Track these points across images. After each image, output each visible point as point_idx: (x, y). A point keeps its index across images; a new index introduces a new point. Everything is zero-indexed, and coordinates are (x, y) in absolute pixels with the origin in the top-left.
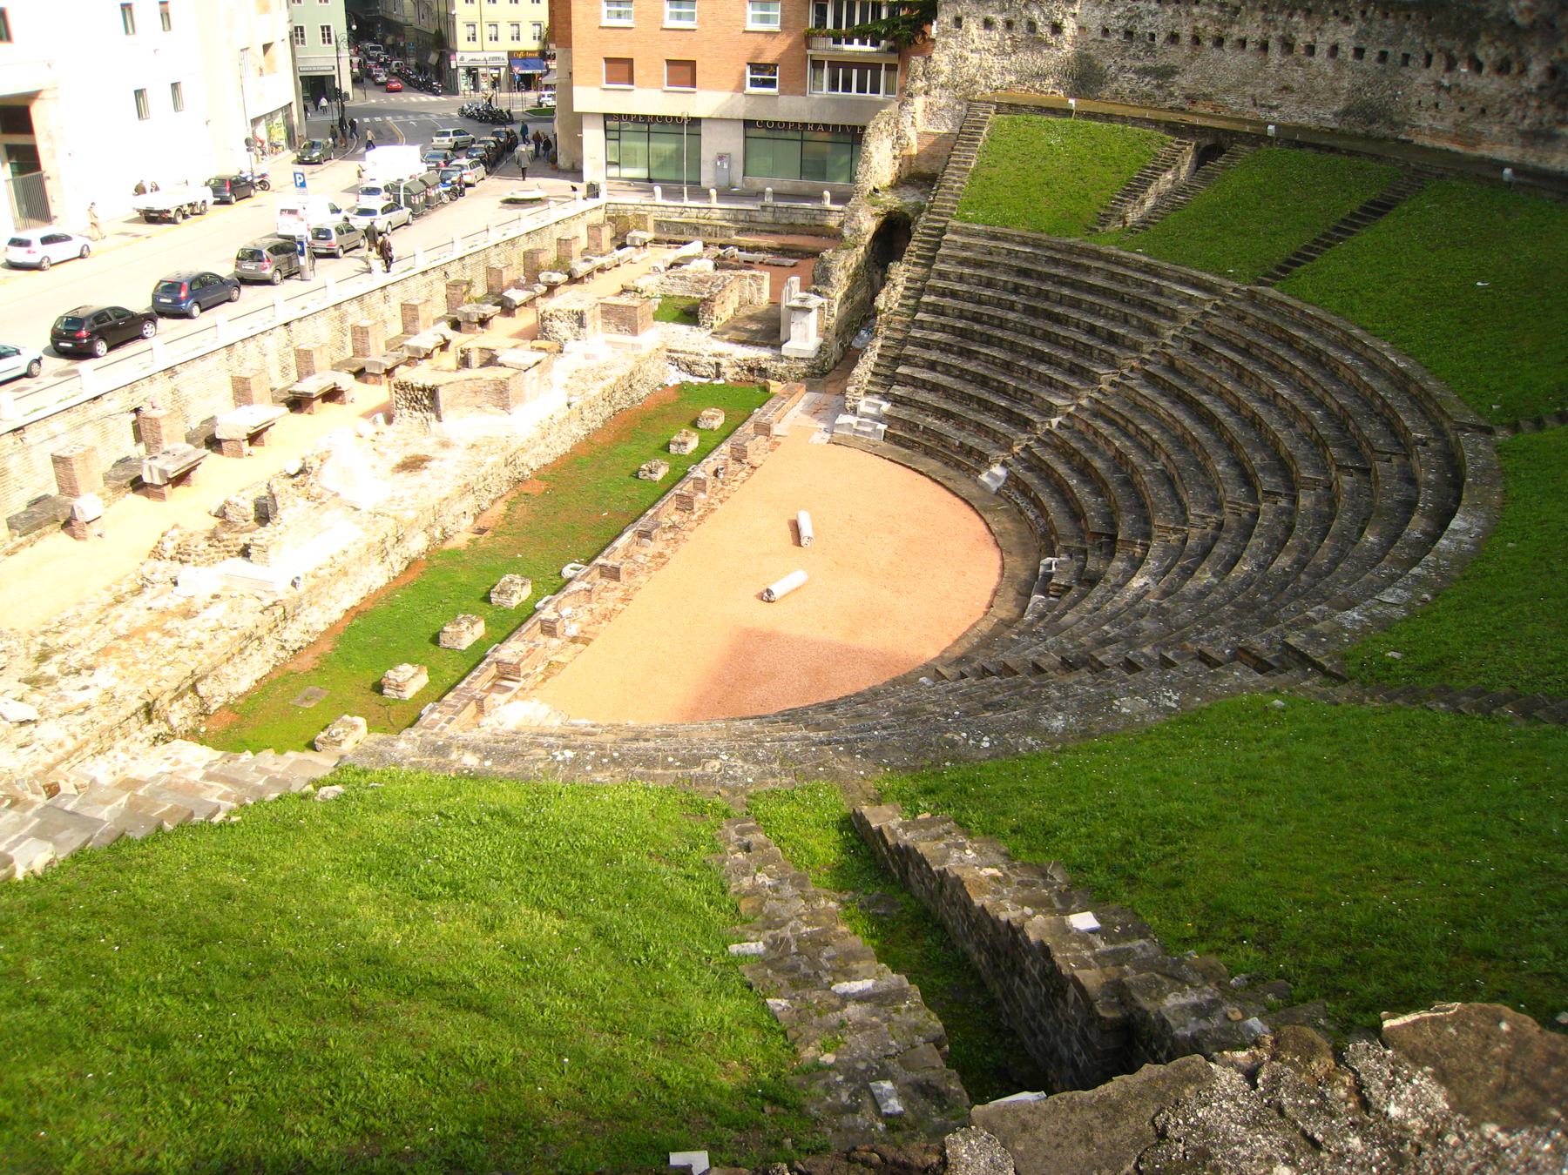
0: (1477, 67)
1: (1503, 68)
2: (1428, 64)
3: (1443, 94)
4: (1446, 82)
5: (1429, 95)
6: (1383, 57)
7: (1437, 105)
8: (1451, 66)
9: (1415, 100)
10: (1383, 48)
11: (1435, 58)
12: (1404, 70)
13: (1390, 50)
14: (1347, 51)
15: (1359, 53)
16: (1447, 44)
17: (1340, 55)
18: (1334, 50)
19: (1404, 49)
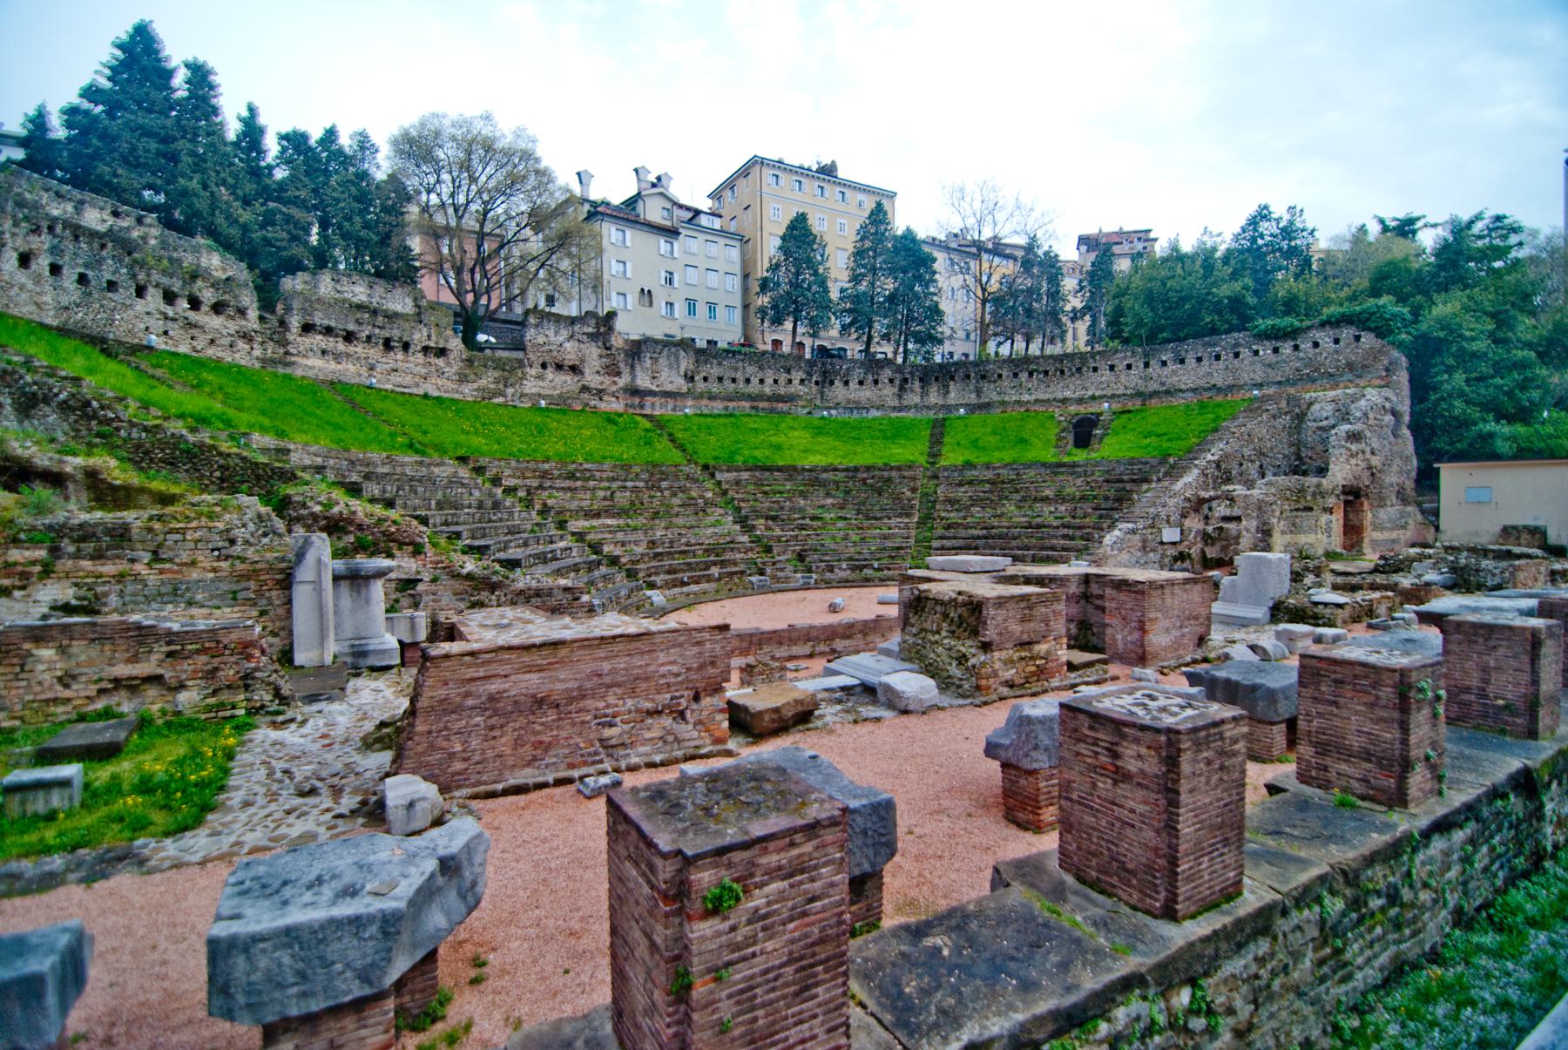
0: (195, 304)
1: (218, 308)
2: (140, 292)
3: (170, 323)
4: (171, 314)
5: (158, 325)
6: (82, 279)
7: (166, 333)
8: (170, 297)
9: (142, 326)
10: (81, 270)
11: (151, 290)
12: (115, 296)
13: (90, 273)
14: (42, 263)
15: (55, 270)
16: (165, 281)
17: (34, 266)
18: (25, 260)
19: (108, 276)
